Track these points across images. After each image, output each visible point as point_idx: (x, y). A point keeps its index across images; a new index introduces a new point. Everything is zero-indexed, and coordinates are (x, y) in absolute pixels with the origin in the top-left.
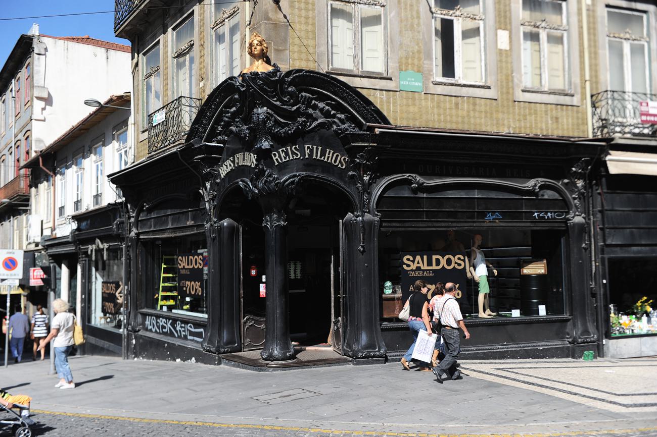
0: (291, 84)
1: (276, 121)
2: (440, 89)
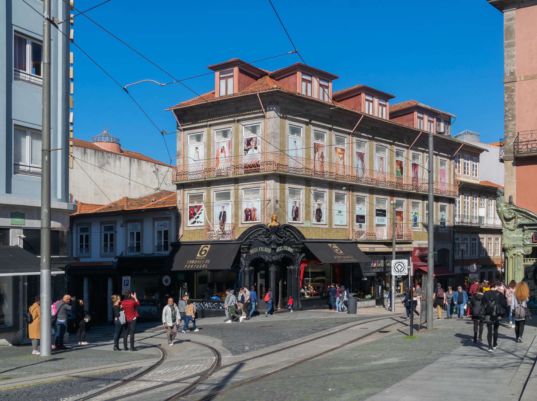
0: (283, 228)
1: (278, 239)
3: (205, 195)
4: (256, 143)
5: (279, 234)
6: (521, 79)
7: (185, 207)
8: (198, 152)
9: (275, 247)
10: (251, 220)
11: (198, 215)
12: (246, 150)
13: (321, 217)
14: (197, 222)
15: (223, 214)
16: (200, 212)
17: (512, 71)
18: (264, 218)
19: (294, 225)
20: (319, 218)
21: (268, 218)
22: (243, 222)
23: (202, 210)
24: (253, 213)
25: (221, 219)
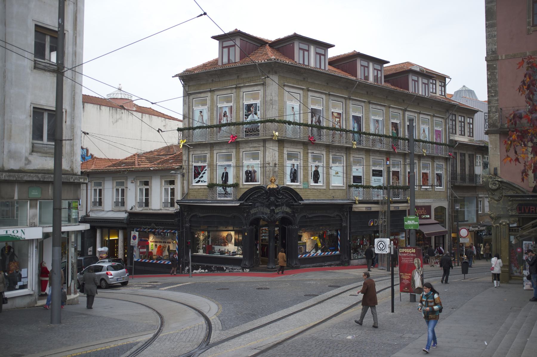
2: (312, 187)
3: (208, 156)
4: (256, 110)
5: (277, 196)
6: (502, 58)
7: (190, 167)
8: (202, 116)
9: (274, 208)
10: (251, 181)
12: (247, 116)
13: (318, 178)
15: (226, 175)
17: (494, 50)
18: (264, 180)
19: (292, 187)
20: (316, 180)
21: (267, 180)
22: (245, 183)
23: (206, 170)
24: (253, 175)
25: (224, 179)
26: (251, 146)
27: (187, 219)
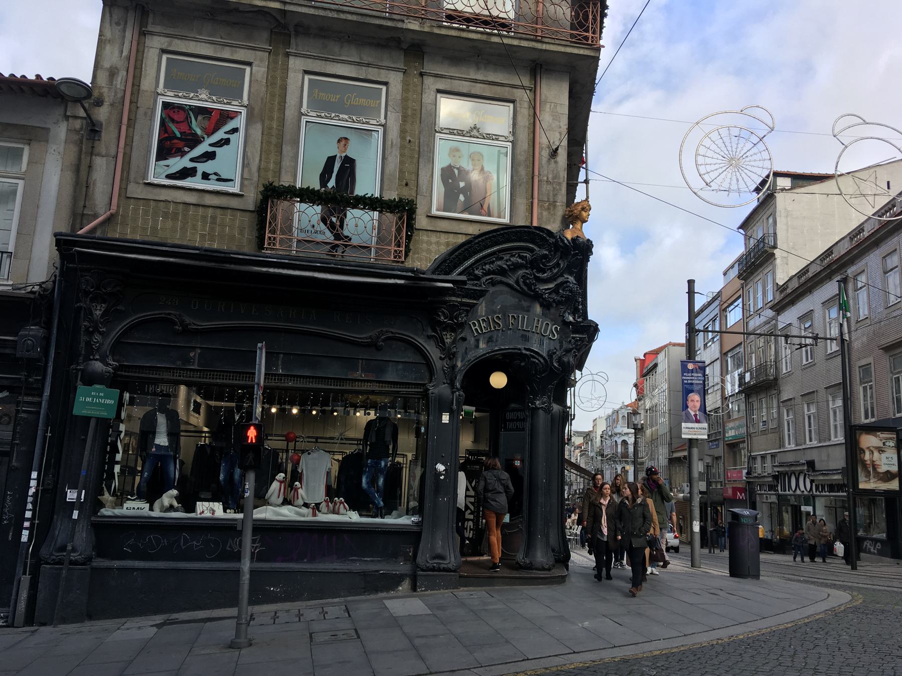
7: (143, 102)
11: (211, 149)
14: (199, 174)
16: (219, 135)
21: (545, 213)
22: (434, 212)
23: (235, 130)
26: (473, 75)
27: (97, 337)
